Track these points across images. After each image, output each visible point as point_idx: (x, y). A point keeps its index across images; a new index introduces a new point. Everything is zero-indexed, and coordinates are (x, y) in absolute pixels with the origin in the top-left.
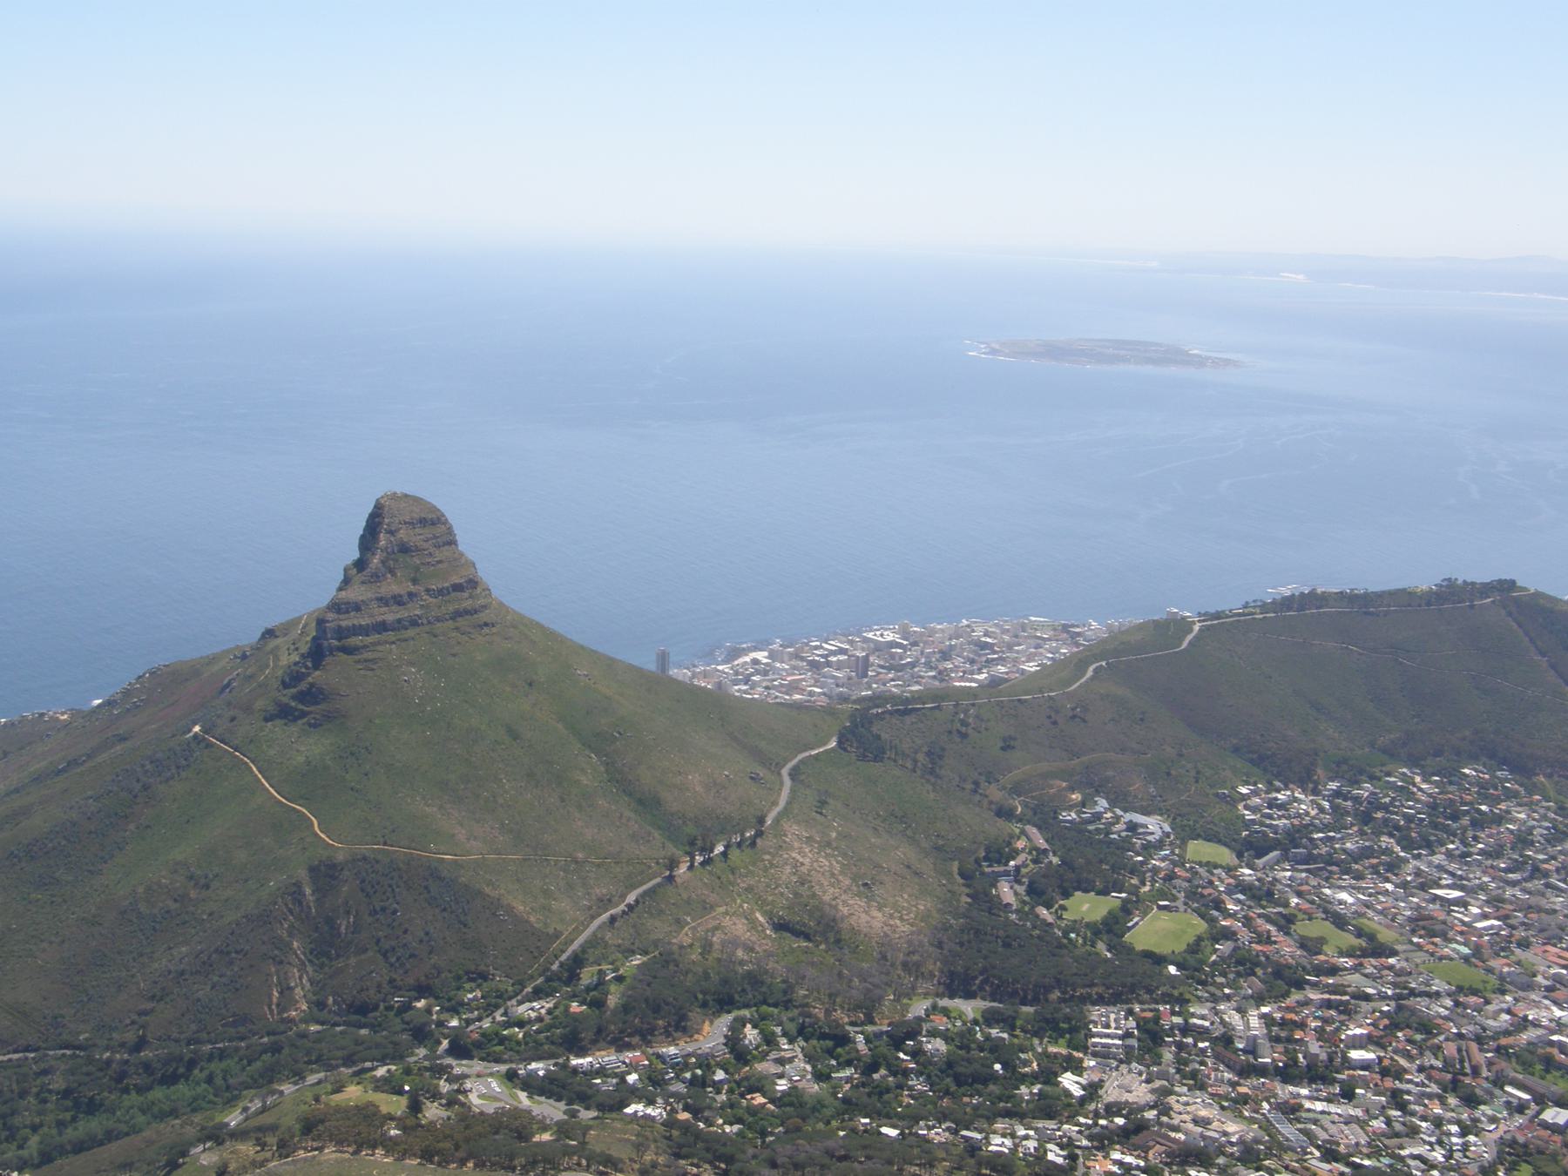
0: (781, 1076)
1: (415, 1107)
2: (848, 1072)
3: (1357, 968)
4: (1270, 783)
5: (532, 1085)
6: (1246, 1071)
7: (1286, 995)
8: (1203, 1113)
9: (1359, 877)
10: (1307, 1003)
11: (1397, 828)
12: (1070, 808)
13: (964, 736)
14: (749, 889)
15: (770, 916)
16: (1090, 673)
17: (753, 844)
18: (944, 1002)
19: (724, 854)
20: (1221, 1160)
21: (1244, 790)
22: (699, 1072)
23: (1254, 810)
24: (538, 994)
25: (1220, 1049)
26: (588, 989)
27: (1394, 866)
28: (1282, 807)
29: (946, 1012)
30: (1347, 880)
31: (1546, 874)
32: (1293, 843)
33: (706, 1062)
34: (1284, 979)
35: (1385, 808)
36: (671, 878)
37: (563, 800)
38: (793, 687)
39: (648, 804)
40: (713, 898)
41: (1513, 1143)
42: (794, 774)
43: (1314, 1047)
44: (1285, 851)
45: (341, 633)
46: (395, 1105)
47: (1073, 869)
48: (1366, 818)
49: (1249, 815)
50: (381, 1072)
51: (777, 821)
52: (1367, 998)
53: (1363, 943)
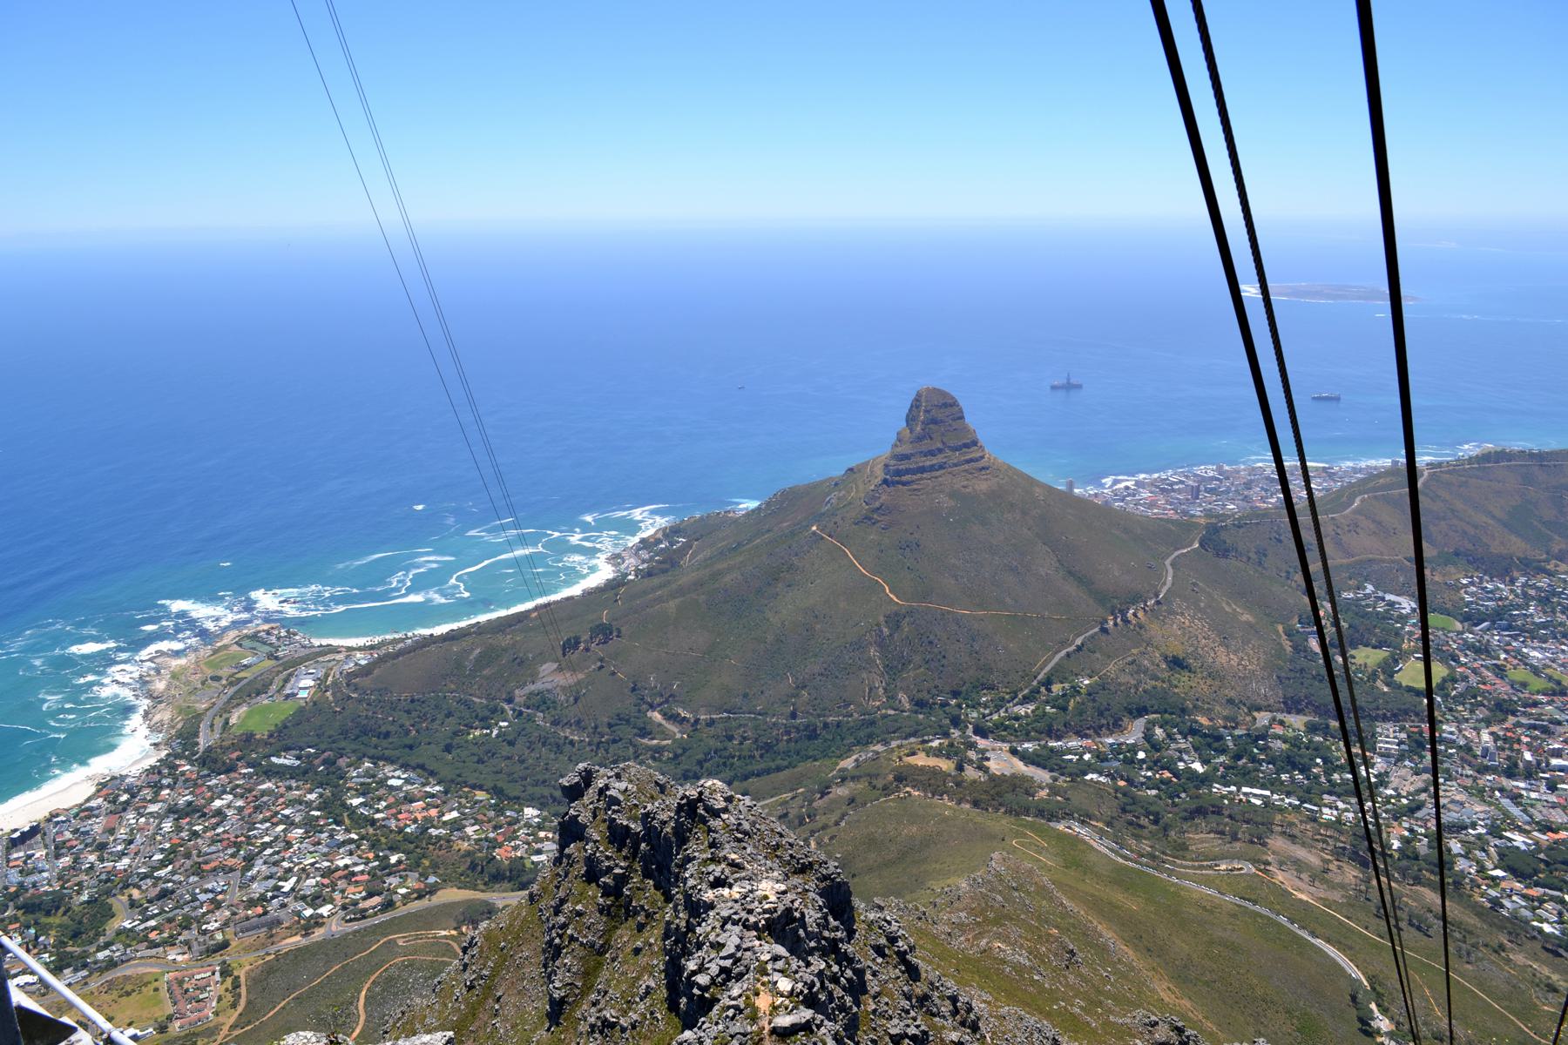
1: (960, 768)
3: (1549, 703)
5: (1026, 758)
6: (1484, 770)
7: (1504, 720)
8: (1458, 798)
10: (1519, 725)
12: (1349, 590)
18: (1279, 716)
21: (1464, 582)
23: (1472, 594)
24: (1026, 700)
25: (1462, 754)
26: (1057, 698)
29: (1282, 723)
30: (1536, 644)
32: (1499, 617)
33: (1134, 749)
34: (1502, 709)
38: (1152, 505)
43: (1528, 756)
44: (1493, 622)
45: (899, 473)
46: (946, 765)
49: (1468, 598)
50: (935, 744)
52: (1559, 723)
53: (1551, 685)
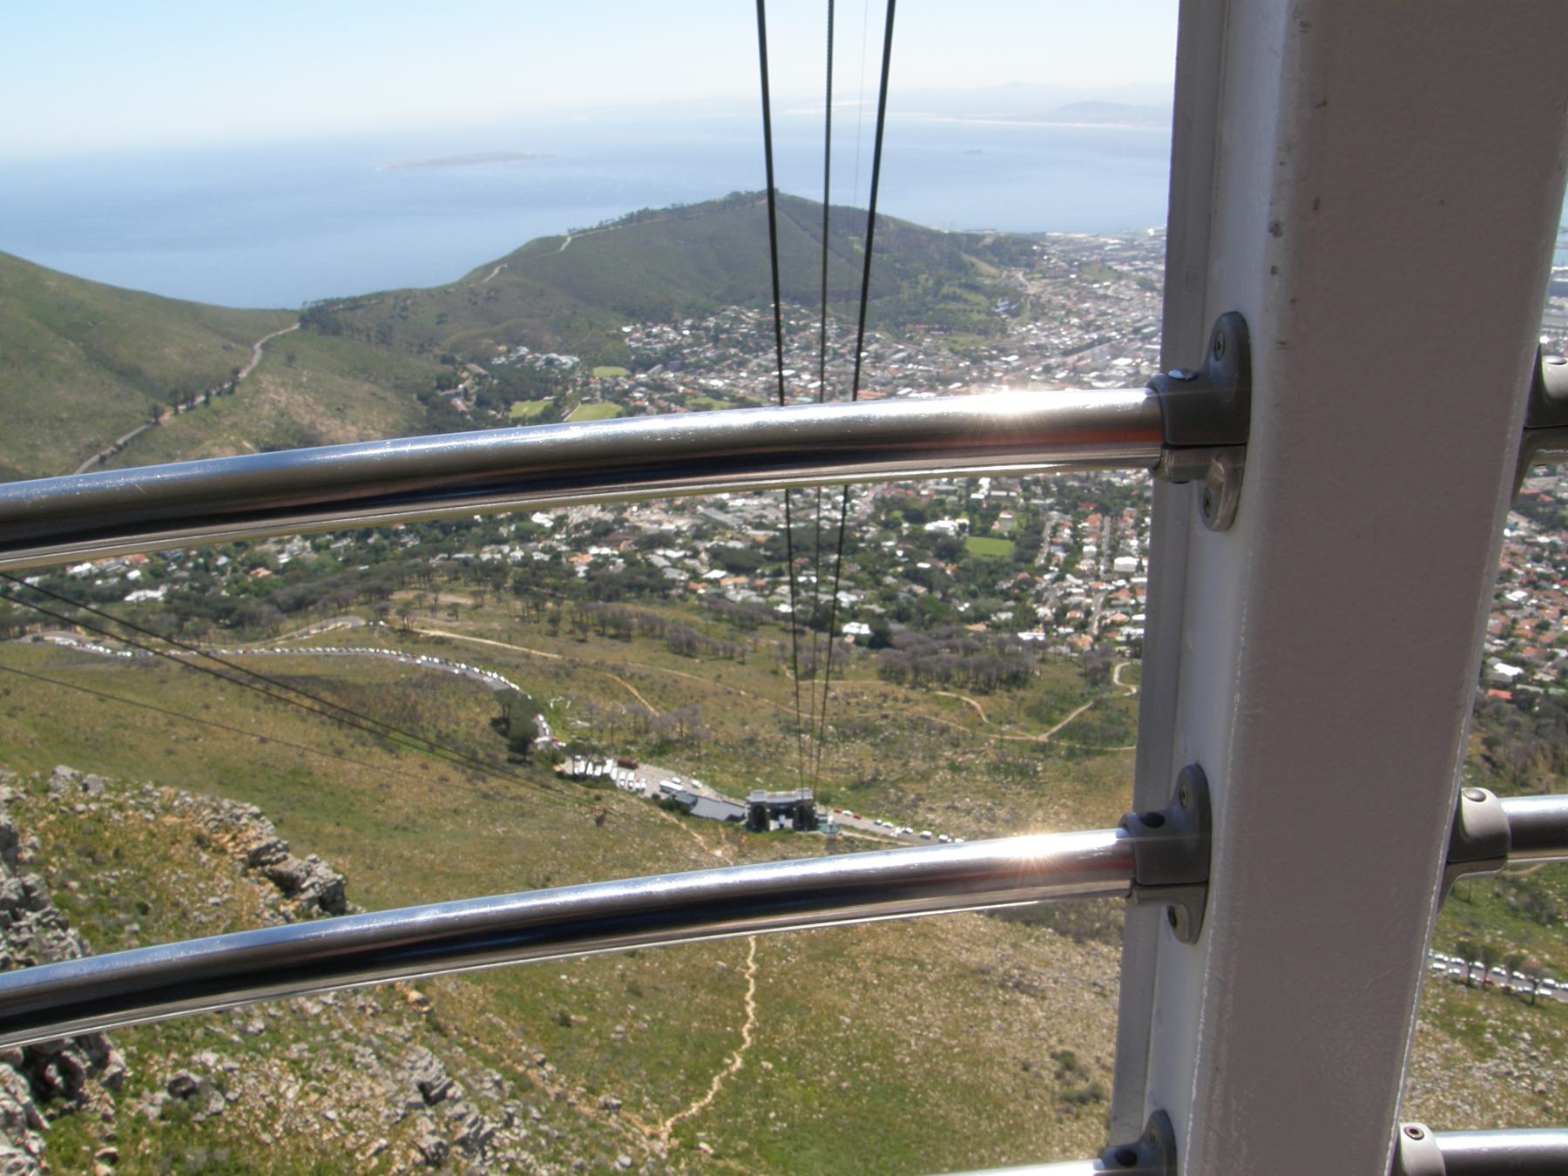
0: (281, 552)
2: (345, 542)
4: (644, 324)
9: (721, 371)
11: (739, 342)
12: (500, 355)
13: (405, 318)
14: (234, 426)
15: (256, 443)
16: (496, 271)
17: (231, 391)
19: (207, 402)
20: (680, 541)
21: (626, 329)
22: (201, 560)
23: (638, 340)
27: (742, 364)
28: (655, 336)
31: (843, 356)
32: (671, 357)
35: (727, 331)
36: (157, 423)
37: (42, 375)
39: (129, 375)
40: (200, 435)
41: (883, 500)
42: (264, 347)
47: (510, 384)
48: (716, 340)
49: (634, 345)
51: (252, 374)
